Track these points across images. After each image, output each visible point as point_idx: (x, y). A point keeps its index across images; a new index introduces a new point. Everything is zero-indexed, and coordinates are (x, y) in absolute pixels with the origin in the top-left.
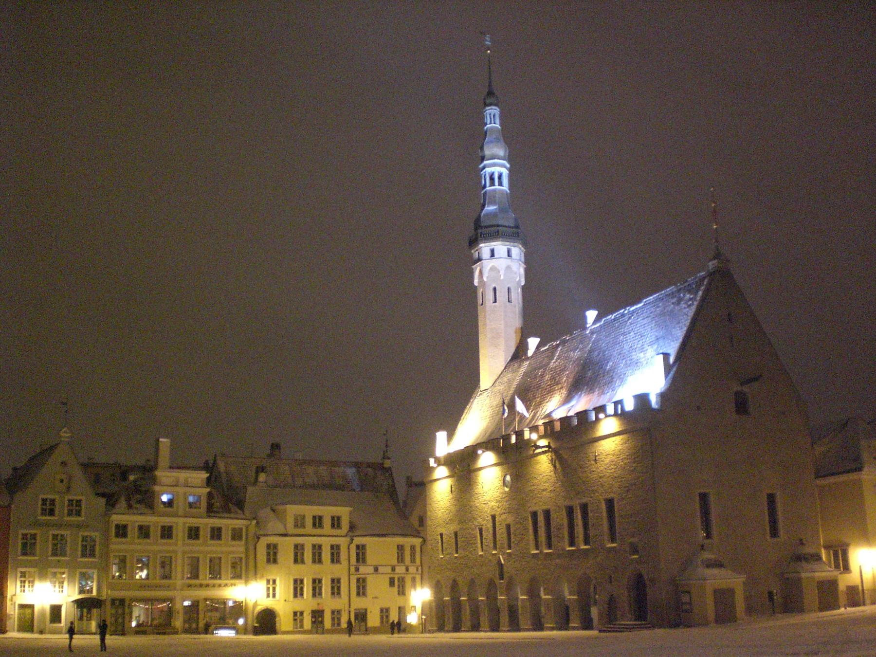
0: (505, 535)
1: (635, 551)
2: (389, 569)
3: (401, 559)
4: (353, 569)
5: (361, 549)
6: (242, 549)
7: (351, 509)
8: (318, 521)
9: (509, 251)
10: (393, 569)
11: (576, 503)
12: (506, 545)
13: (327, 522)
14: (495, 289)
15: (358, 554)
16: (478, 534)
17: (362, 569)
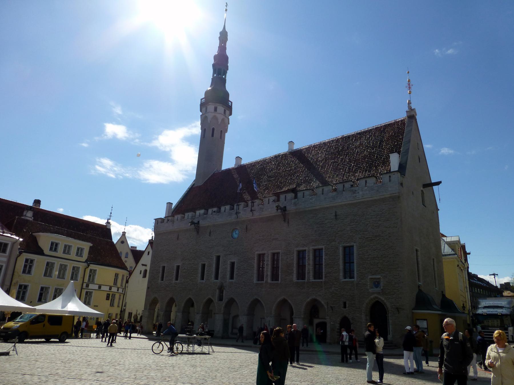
0: (229, 269)
1: (377, 284)
2: (107, 289)
3: (115, 283)
4: (85, 285)
6: (5, 259)
7: (92, 245)
8: (67, 249)
9: (225, 111)
10: (110, 289)
11: (309, 250)
12: (228, 276)
13: (74, 251)
14: (213, 129)
15: (90, 276)
16: (200, 269)
17: (91, 286)
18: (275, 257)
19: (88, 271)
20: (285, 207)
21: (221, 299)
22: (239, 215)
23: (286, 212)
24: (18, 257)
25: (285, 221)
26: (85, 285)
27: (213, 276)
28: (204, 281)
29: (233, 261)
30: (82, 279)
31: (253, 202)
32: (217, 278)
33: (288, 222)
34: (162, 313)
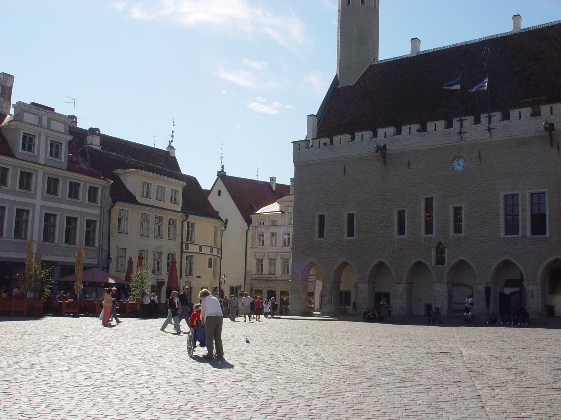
5: (191, 226)
6: (97, 212)
7: (185, 184)
12: (452, 228)
15: (188, 231)
17: (193, 248)
18: (537, 199)
19: (185, 224)
20: (552, 125)
21: (440, 261)
22: (463, 136)
23: (553, 132)
24: (111, 208)
25: (552, 145)
26: (184, 245)
27: (423, 228)
28: (405, 236)
29: (458, 205)
30: (180, 237)
31: (490, 117)
32: (429, 229)
33: (558, 147)
34: (331, 284)
